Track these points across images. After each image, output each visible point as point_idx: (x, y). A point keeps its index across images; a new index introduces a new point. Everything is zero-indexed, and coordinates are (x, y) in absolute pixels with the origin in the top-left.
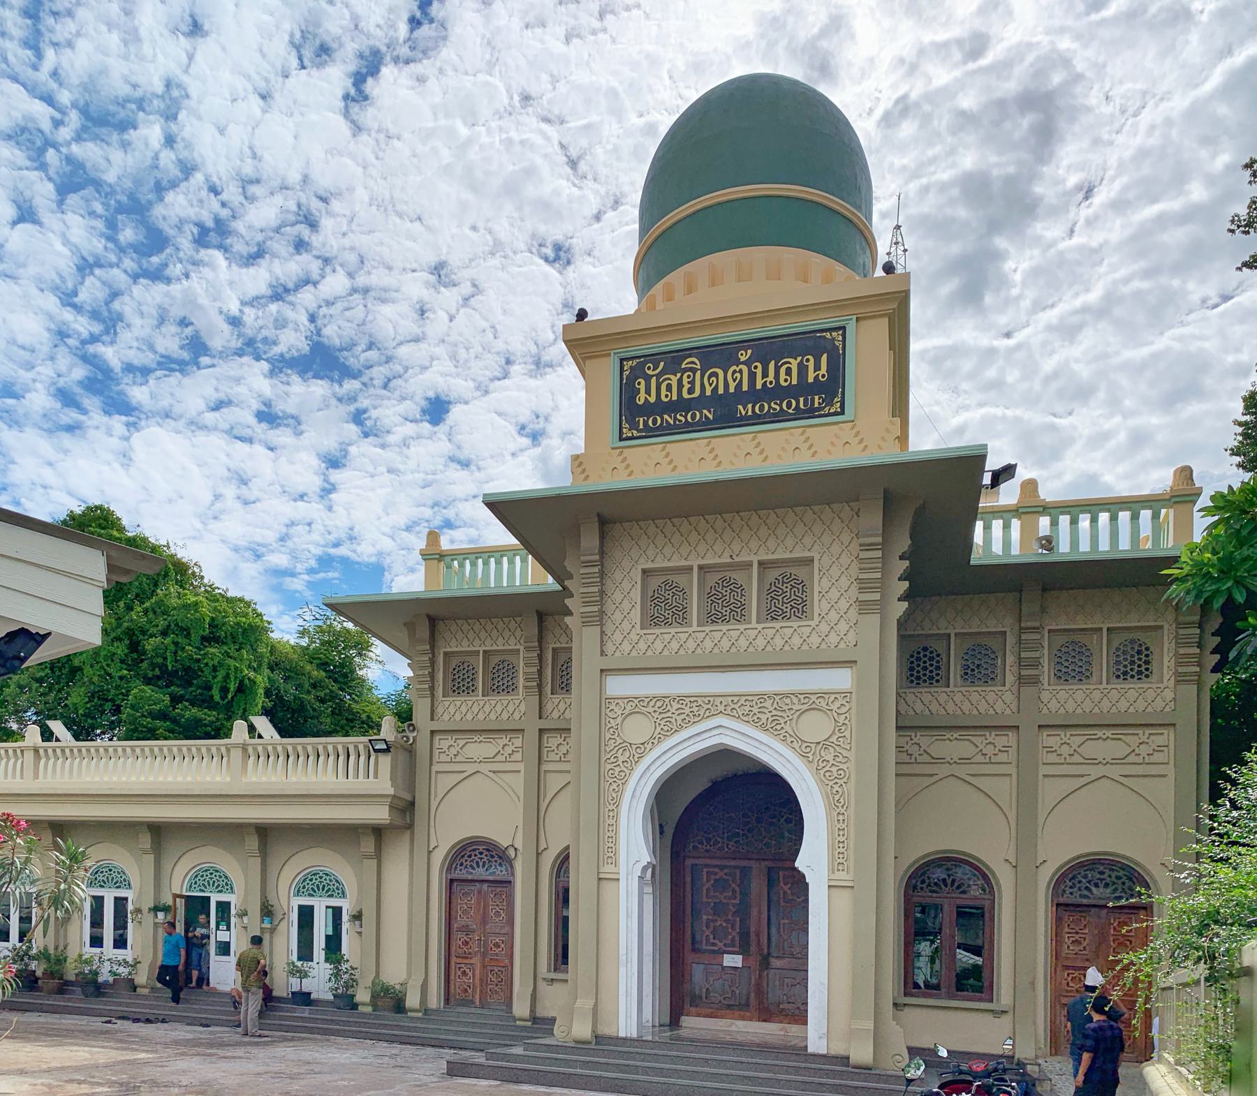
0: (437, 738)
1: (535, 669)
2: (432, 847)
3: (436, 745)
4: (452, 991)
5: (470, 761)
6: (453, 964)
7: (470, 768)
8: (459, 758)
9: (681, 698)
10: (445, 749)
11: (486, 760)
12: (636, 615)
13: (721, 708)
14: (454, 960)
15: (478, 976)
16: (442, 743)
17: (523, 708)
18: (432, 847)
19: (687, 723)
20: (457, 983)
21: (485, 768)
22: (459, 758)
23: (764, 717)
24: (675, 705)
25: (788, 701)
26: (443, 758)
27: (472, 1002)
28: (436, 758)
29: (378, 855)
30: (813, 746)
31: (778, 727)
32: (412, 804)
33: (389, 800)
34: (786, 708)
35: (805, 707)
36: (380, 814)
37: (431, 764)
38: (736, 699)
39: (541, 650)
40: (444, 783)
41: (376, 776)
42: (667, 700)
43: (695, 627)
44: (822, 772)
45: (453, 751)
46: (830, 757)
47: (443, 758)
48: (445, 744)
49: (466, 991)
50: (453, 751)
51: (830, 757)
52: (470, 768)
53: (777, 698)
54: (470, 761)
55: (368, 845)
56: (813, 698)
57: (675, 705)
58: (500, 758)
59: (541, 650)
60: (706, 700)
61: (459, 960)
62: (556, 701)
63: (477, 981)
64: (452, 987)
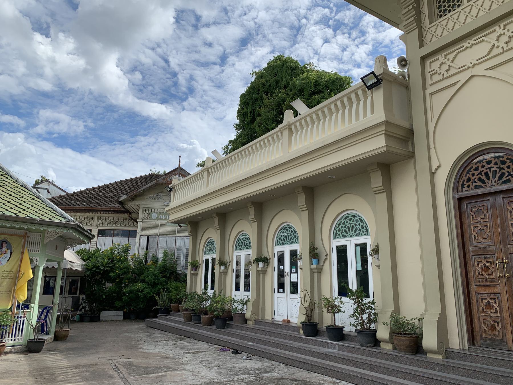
0: (428, 63)
2: (434, 167)
3: (428, 69)
4: (477, 328)
5: (463, 69)
6: (473, 295)
7: (463, 77)
8: (451, 73)
10: (437, 69)
11: (481, 61)
14: (474, 289)
15: (506, 309)
16: (432, 66)
18: (434, 167)
20: (482, 317)
21: (479, 70)
22: (451, 73)
26: (436, 78)
27: (503, 342)
28: (429, 81)
29: (388, 188)
32: (411, 132)
33: (383, 128)
36: (377, 144)
37: (425, 88)
40: (438, 102)
41: (372, 112)
45: (445, 67)
47: (436, 78)
48: (435, 66)
49: (493, 328)
50: (445, 67)
52: (463, 77)
54: (463, 69)
55: (377, 180)
58: (495, 51)
61: (482, 290)
63: (506, 315)
64: (476, 321)
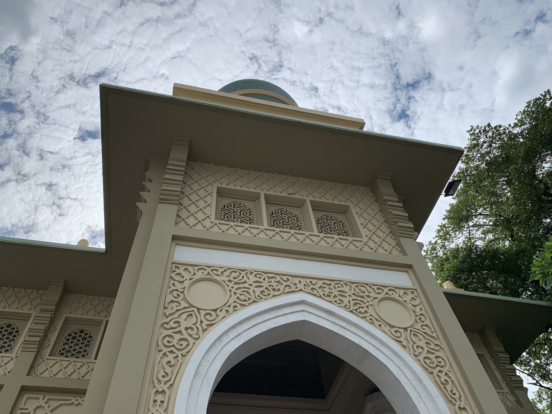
1: (43, 327)
9: (258, 273)
12: (212, 211)
13: (300, 286)
17: (10, 366)
19: (264, 296)
23: (346, 300)
24: (252, 278)
25: (363, 289)
30: (402, 331)
31: (363, 310)
34: (362, 294)
35: (380, 296)
38: (314, 281)
39: (55, 314)
42: (243, 273)
43: (266, 226)
44: (421, 358)
46: (422, 344)
51: (422, 344)
53: (353, 286)
56: (386, 290)
57: (252, 278)
59: (55, 314)
60: (285, 278)
62: (51, 363)
